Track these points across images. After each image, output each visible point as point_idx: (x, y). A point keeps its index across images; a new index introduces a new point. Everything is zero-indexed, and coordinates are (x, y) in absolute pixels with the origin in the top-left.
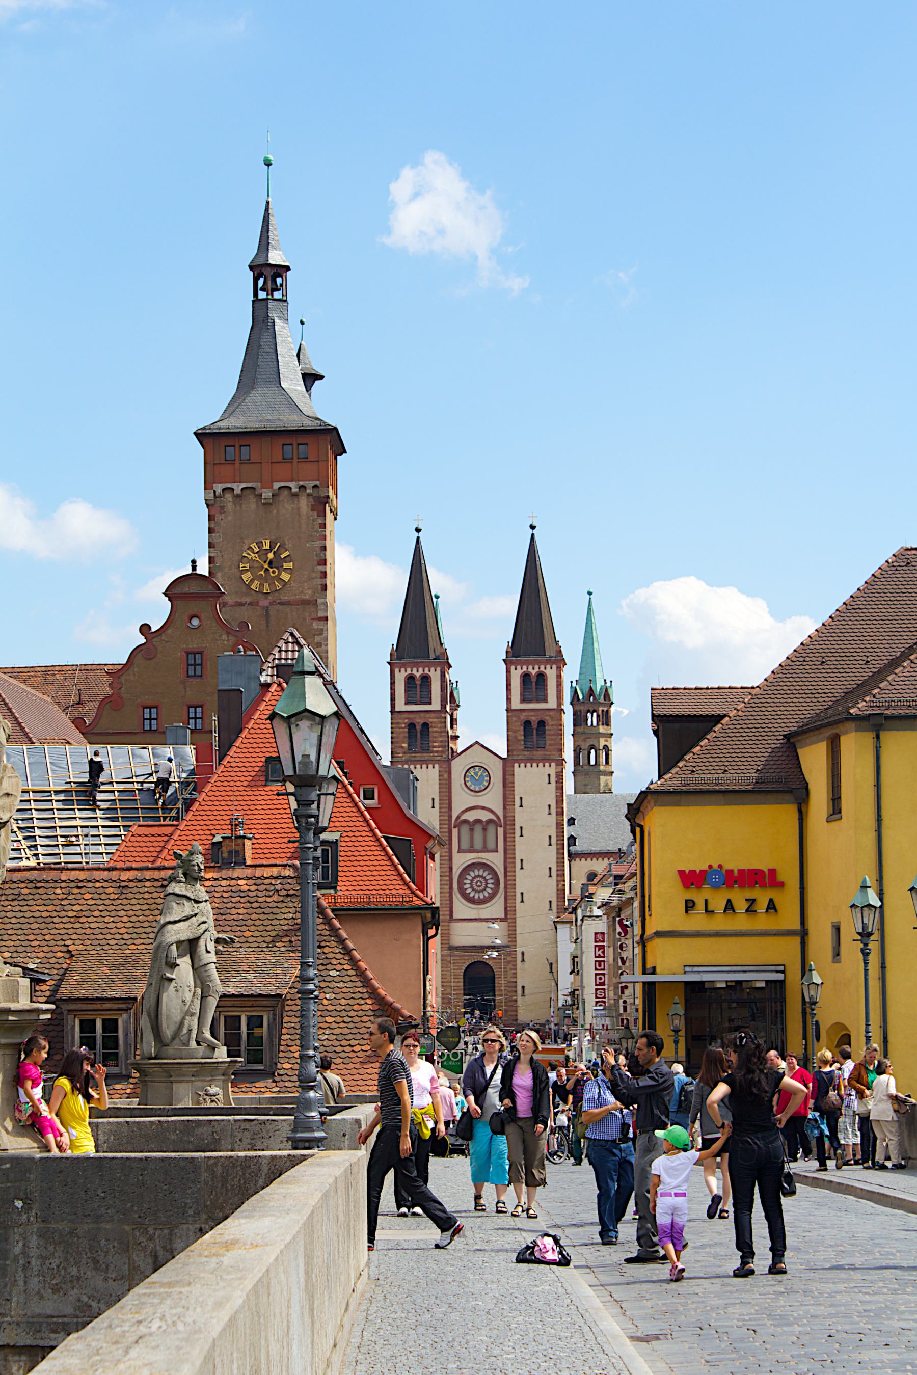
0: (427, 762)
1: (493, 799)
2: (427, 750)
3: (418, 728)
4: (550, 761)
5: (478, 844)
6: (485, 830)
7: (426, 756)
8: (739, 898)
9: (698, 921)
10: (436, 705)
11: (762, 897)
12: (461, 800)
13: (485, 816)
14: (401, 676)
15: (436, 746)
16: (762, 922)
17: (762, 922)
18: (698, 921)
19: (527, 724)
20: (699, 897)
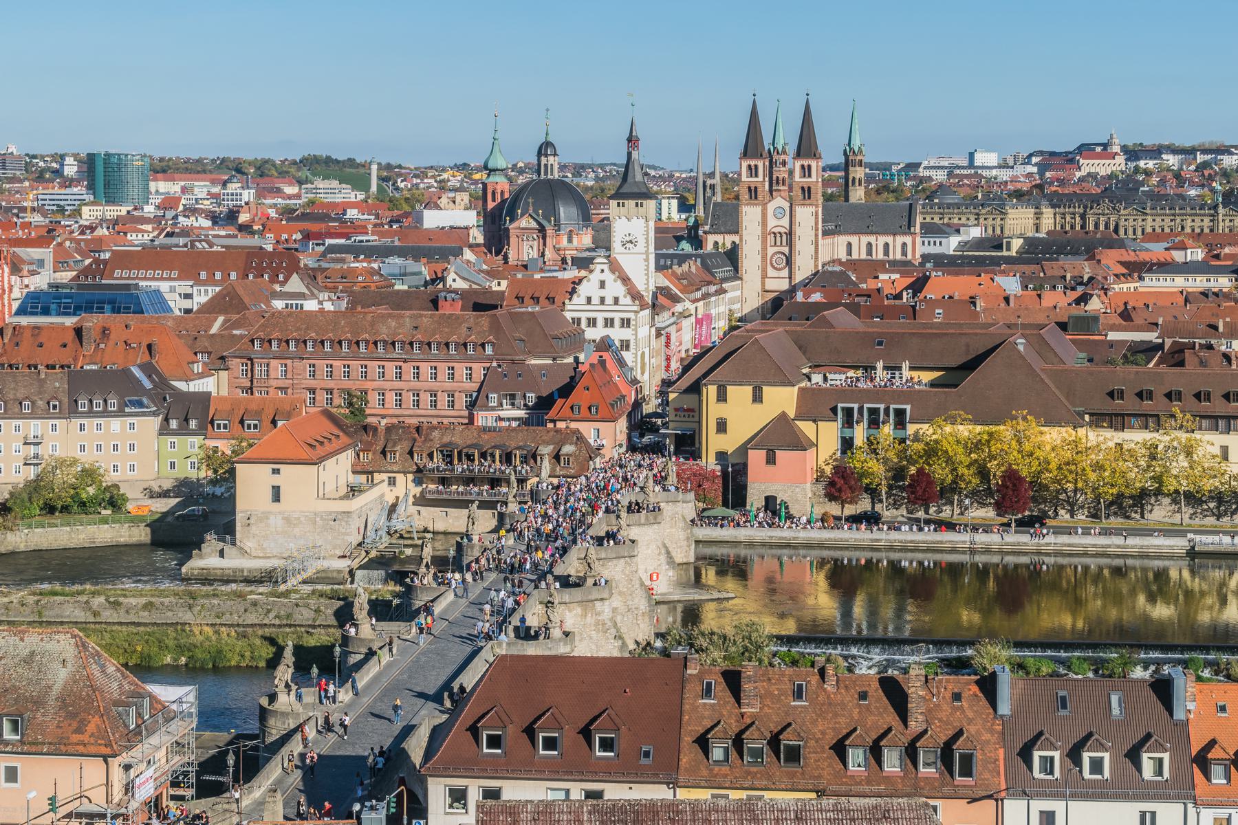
0: (756, 204)
1: (785, 222)
2: (756, 198)
3: (753, 189)
4: (812, 205)
5: (778, 243)
6: (781, 237)
7: (756, 202)
8: (686, 414)
9: (677, 419)
10: (760, 178)
11: (691, 414)
12: (772, 222)
13: (783, 230)
14: (745, 164)
15: (760, 197)
16: (691, 419)
17: (691, 419)
18: (677, 419)
19: (803, 188)
20: (678, 413)
